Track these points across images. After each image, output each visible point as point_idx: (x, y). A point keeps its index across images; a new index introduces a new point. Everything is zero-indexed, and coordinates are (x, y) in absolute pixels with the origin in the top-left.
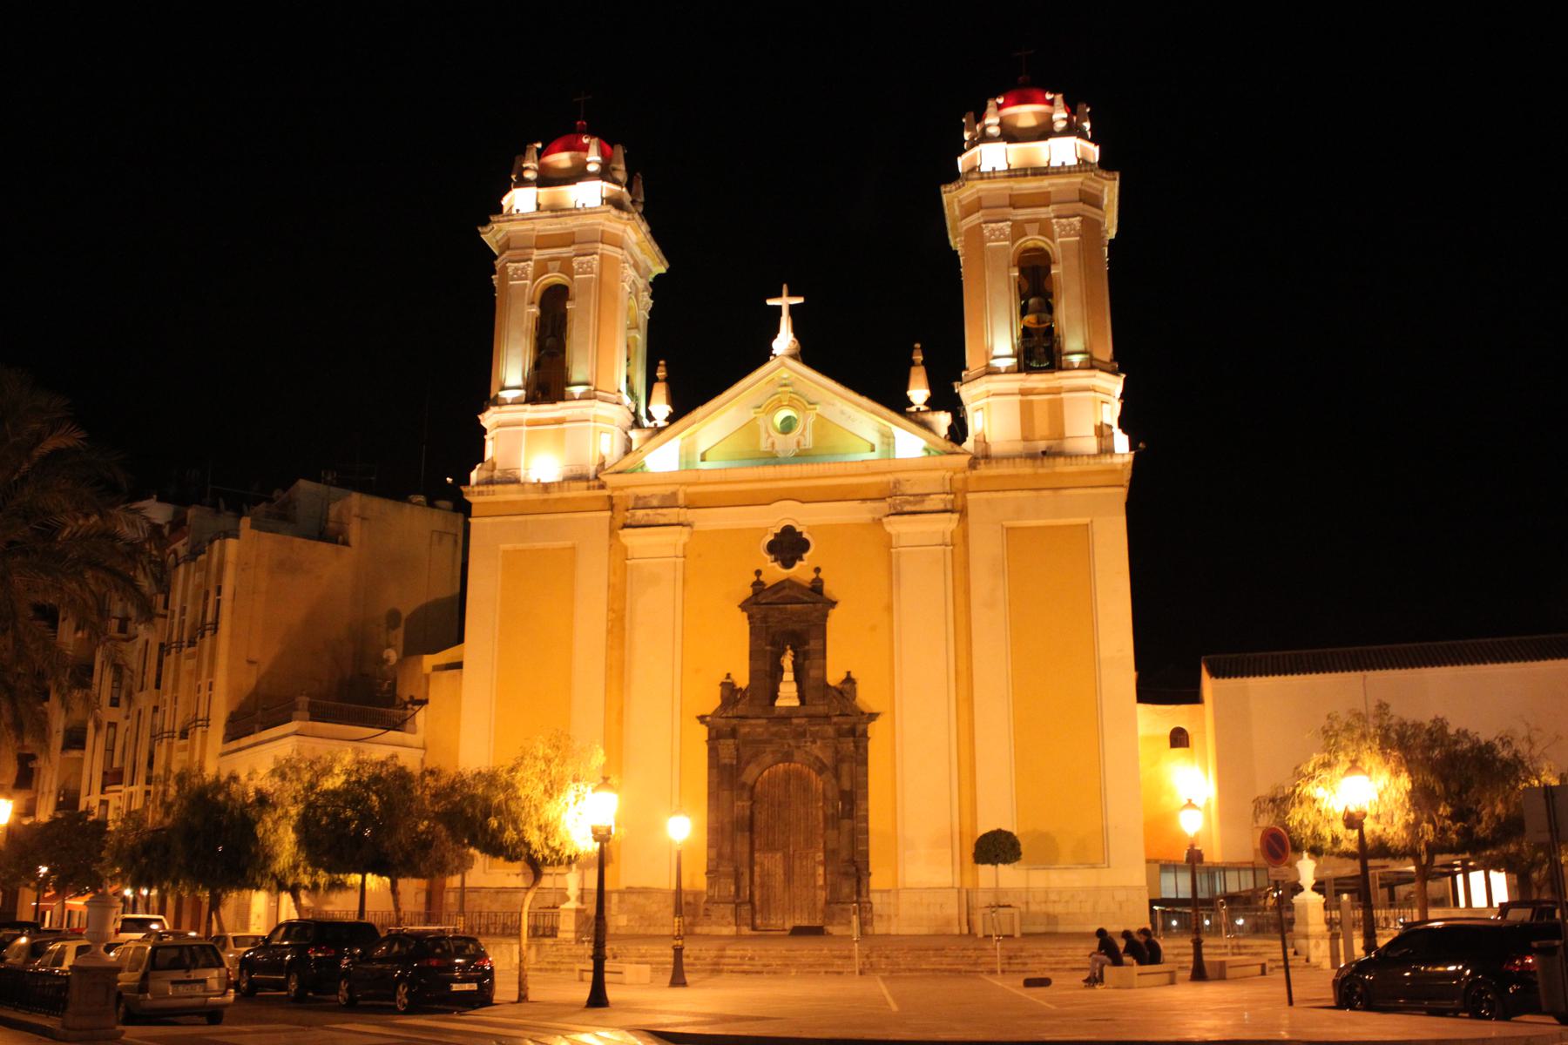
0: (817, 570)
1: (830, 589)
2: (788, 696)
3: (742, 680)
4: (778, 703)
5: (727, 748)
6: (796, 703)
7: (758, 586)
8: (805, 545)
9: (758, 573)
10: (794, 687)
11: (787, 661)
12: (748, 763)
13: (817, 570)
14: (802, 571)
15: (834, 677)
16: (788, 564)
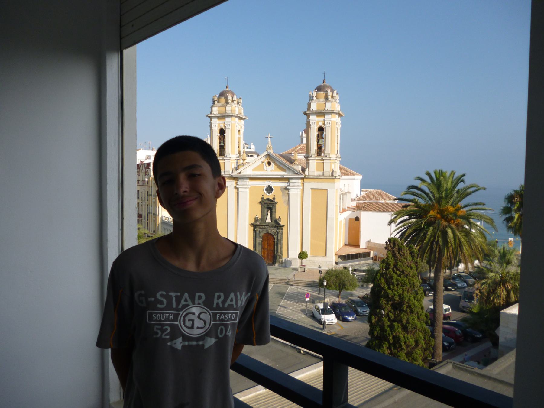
0: (274, 196)
1: (276, 201)
2: (269, 220)
3: (259, 217)
4: (266, 221)
5: (257, 230)
6: (270, 222)
7: (262, 198)
8: (272, 190)
9: (263, 195)
10: (270, 218)
11: (269, 213)
12: (261, 232)
13: (274, 196)
14: (270, 196)
15: (277, 217)
16: (269, 193)
